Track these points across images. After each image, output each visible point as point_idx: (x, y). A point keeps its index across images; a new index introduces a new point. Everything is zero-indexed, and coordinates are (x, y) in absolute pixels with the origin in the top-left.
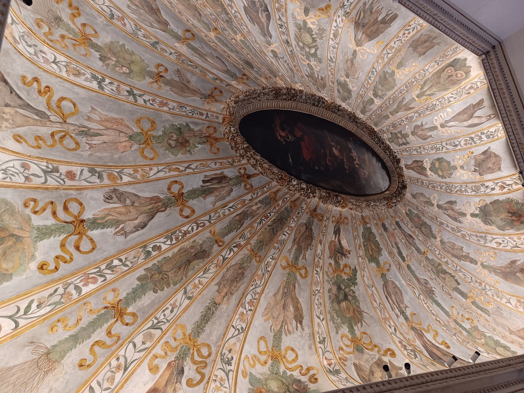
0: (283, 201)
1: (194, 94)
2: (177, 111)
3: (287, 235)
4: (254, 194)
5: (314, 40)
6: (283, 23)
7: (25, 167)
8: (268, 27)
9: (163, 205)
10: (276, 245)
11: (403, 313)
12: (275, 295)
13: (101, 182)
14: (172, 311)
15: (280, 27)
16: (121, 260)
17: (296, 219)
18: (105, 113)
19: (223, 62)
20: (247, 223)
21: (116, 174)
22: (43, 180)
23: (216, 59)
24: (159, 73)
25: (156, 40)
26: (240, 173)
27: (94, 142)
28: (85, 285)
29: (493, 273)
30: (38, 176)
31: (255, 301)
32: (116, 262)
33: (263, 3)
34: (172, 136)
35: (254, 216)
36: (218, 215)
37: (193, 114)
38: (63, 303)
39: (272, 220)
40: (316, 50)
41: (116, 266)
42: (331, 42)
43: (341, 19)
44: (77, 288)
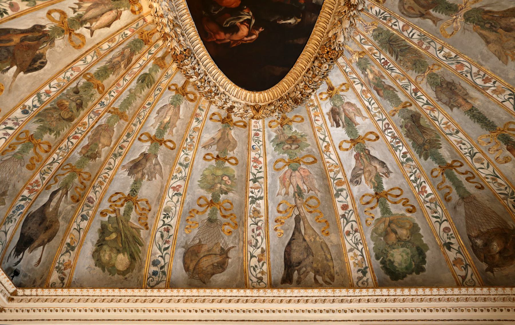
0: (365, 43)
1: (228, 134)
2: (262, 152)
3: (414, 31)
4: (354, 82)
7: (348, 233)
9: (362, 151)
10: (424, 46)
12: (488, 43)
13: (345, 190)
14: (464, 144)
16: (411, 176)
17: (394, 21)
18: (279, 188)
19: (162, 108)
20: (388, 82)
21: (335, 182)
22: (354, 223)
23: (160, 114)
26: (327, 98)
27: (306, 188)
28: (426, 192)
30: (352, 225)
31: (486, 76)
32: (413, 178)
35: (382, 76)
36: (377, 114)
37: (260, 141)
38: (436, 202)
39: (389, 56)
41: (415, 177)
44: (427, 196)
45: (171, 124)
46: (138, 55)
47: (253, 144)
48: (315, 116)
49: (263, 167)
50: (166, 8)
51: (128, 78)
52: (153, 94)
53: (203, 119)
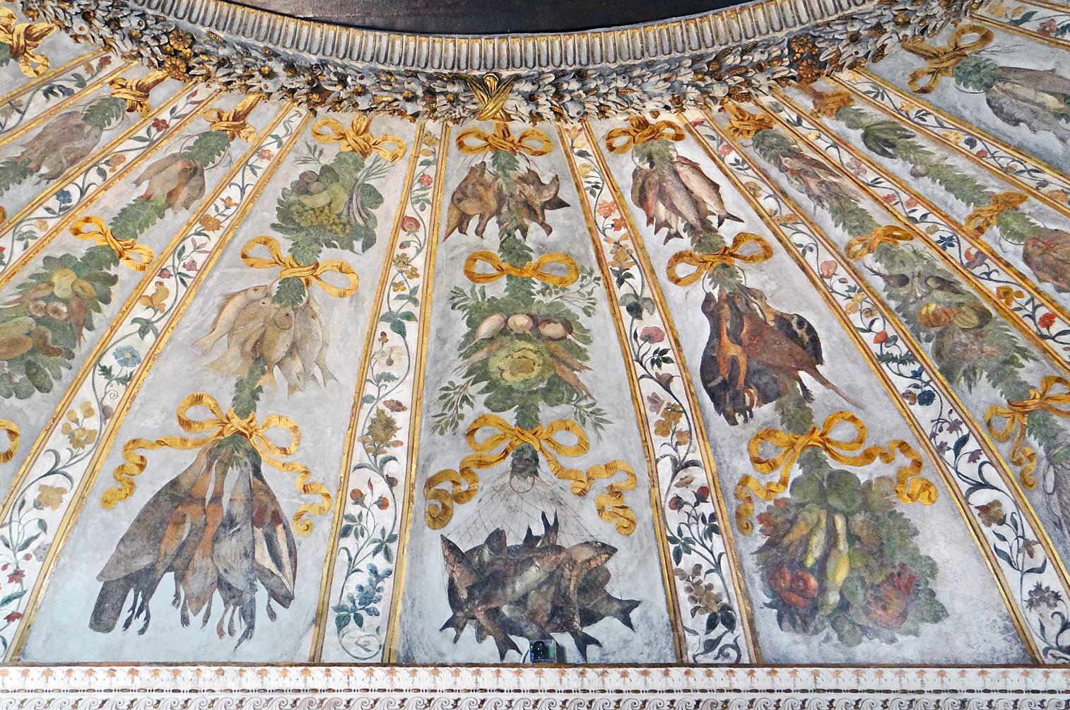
5: (479, 373)
6: (654, 370)
40: (470, 336)
42: (403, 393)
43: (368, 500)
46: (801, 145)
50: (661, 84)
51: (870, 177)
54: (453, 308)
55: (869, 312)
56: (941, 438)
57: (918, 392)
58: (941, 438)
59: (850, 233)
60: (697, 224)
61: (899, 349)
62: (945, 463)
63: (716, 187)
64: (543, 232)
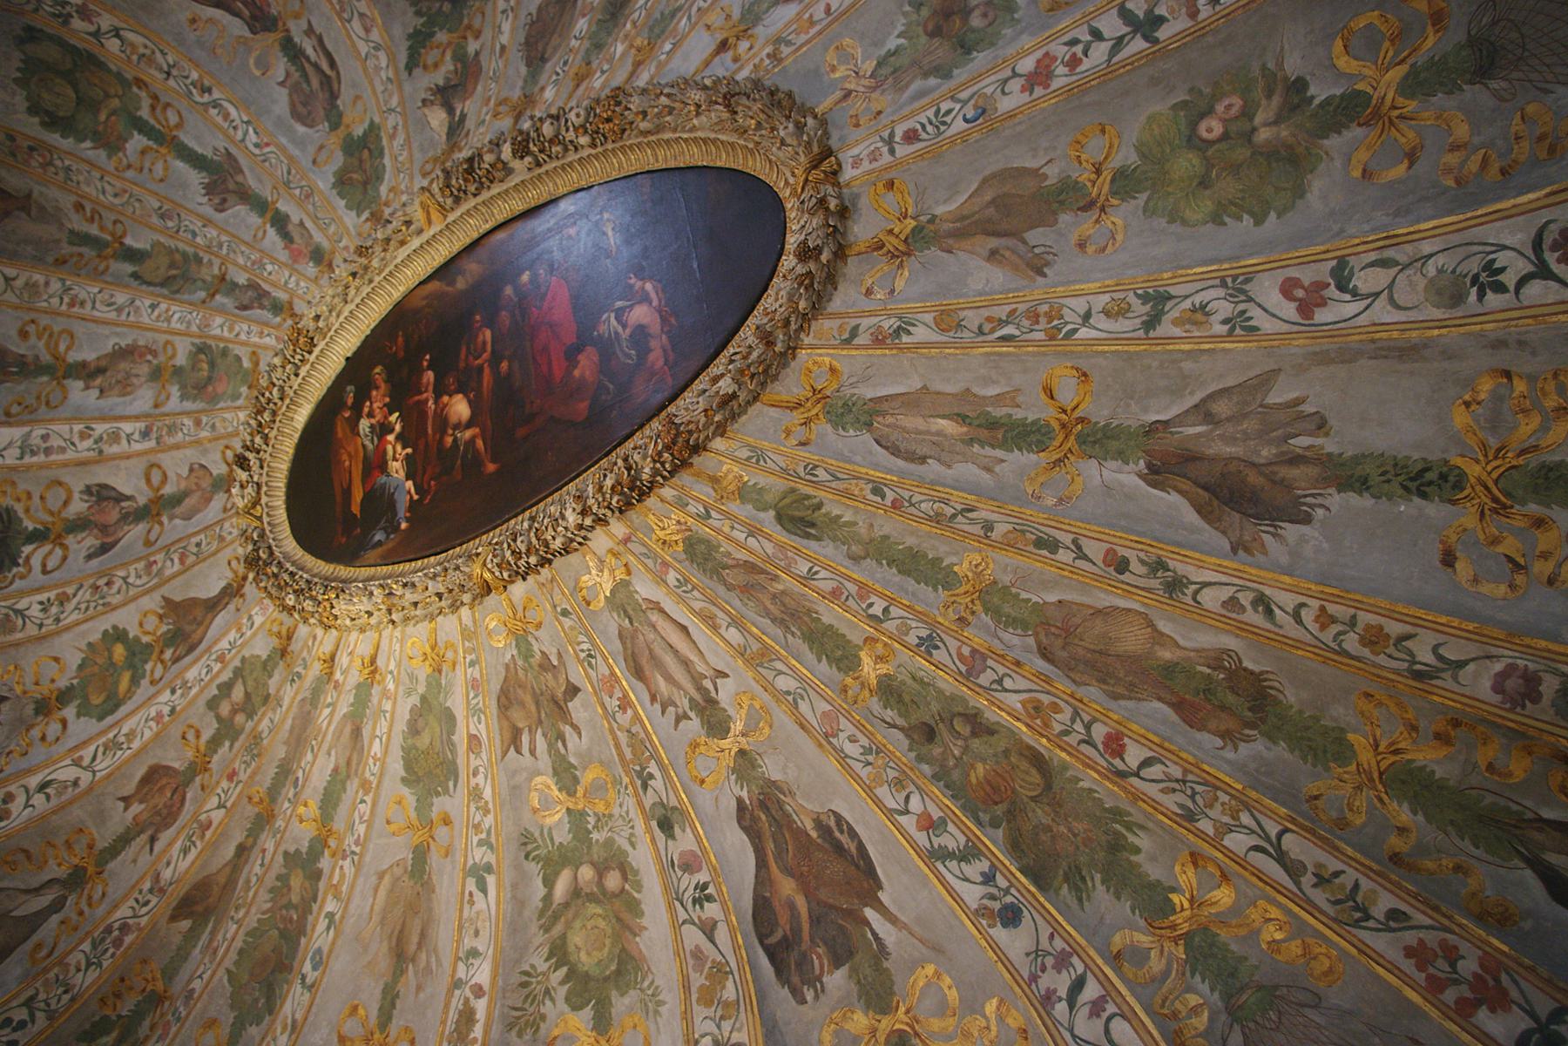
1: (964, 218)
8: (761, 863)
11: (293, 52)
15: (705, 886)
19: (895, 451)
23: (922, 450)
24: (1103, 209)
25: (1160, 331)
29: (30, 359)
33: (796, 979)
34: (985, 15)
40: (548, 898)
42: (482, 974)
45: (966, 410)
47: (960, 125)
48: (812, 23)
49: (1066, 38)
52: (833, 485)
53: (889, 316)
54: (527, 857)
55: (898, 784)
56: (1045, 982)
57: (997, 905)
58: (1045, 982)
59: (839, 669)
60: (697, 697)
61: (952, 839)
62: (1055, 1022)
63: (684, 629)
64: (576, 736)
